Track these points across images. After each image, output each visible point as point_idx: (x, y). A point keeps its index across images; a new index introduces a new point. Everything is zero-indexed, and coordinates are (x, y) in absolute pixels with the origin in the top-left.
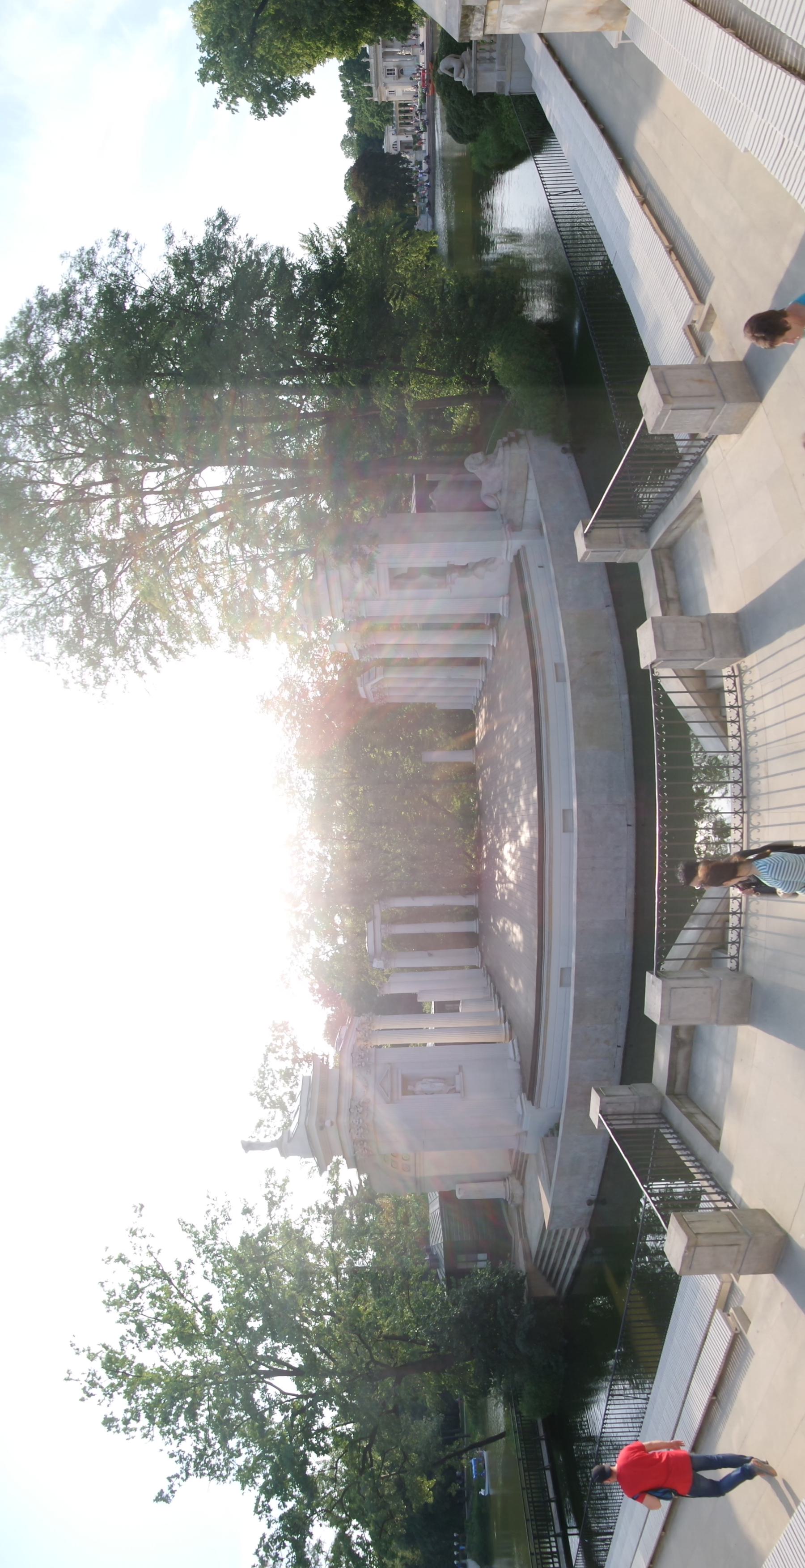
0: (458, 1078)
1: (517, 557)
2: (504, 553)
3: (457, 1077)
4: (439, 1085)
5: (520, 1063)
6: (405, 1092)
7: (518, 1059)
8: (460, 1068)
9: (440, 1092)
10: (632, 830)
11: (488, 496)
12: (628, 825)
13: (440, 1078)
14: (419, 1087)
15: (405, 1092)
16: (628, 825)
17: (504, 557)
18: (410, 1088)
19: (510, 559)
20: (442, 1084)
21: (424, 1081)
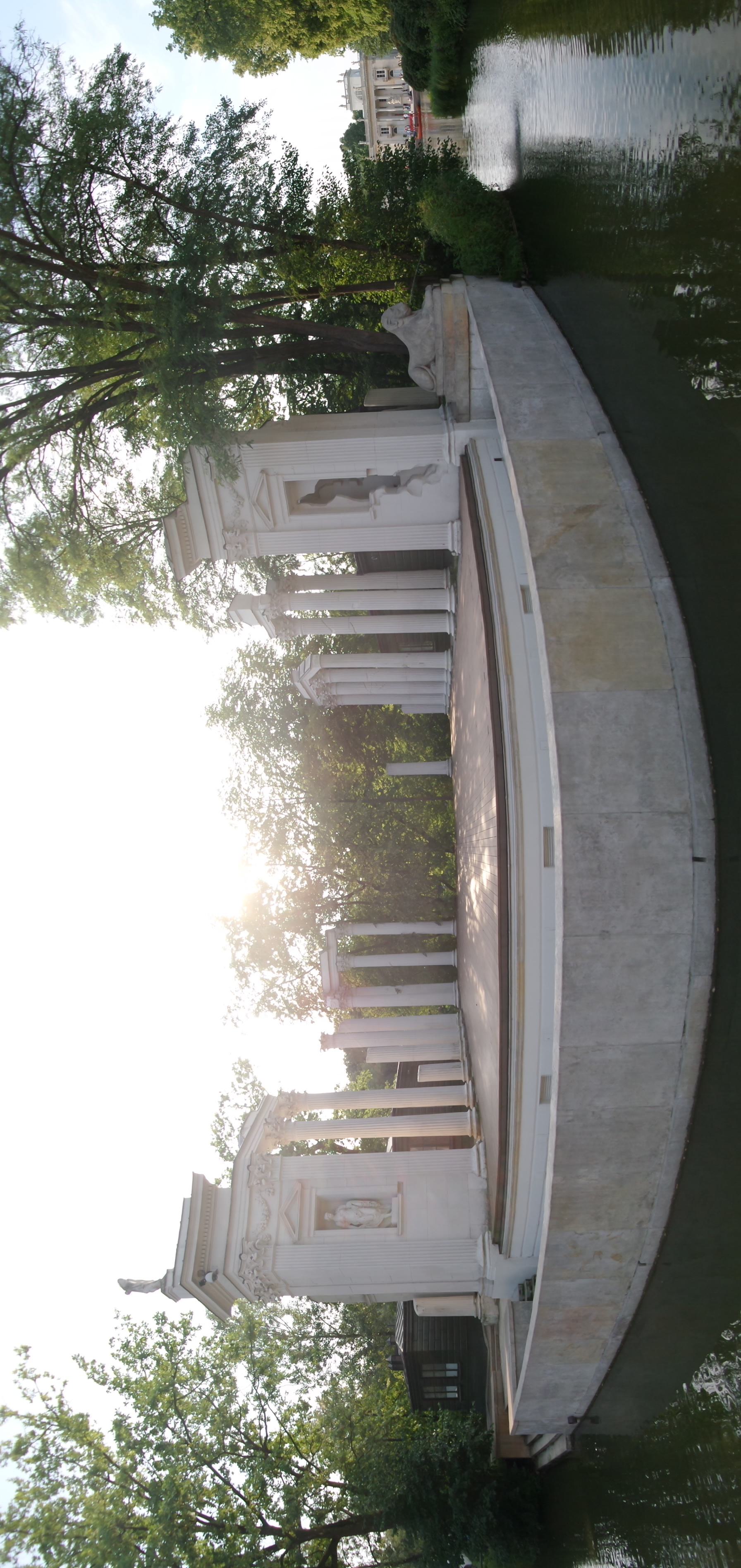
1: (465, 459)
2: (445, 452)
3: (395, 1200)
4: (369, 1214)
5: (487, 1179)
7: (484, 1175)
9: (369, 1225)
10: (707, 870)
11: (419, 368)
12: (696, 859)
13: (370, 1200)
15: (322, 1225)
16: (696, 859)
17: (447, 459)
18: (328, 1216)
19: (457, 461)
20: (373, 1211)
21: (349, 1204)
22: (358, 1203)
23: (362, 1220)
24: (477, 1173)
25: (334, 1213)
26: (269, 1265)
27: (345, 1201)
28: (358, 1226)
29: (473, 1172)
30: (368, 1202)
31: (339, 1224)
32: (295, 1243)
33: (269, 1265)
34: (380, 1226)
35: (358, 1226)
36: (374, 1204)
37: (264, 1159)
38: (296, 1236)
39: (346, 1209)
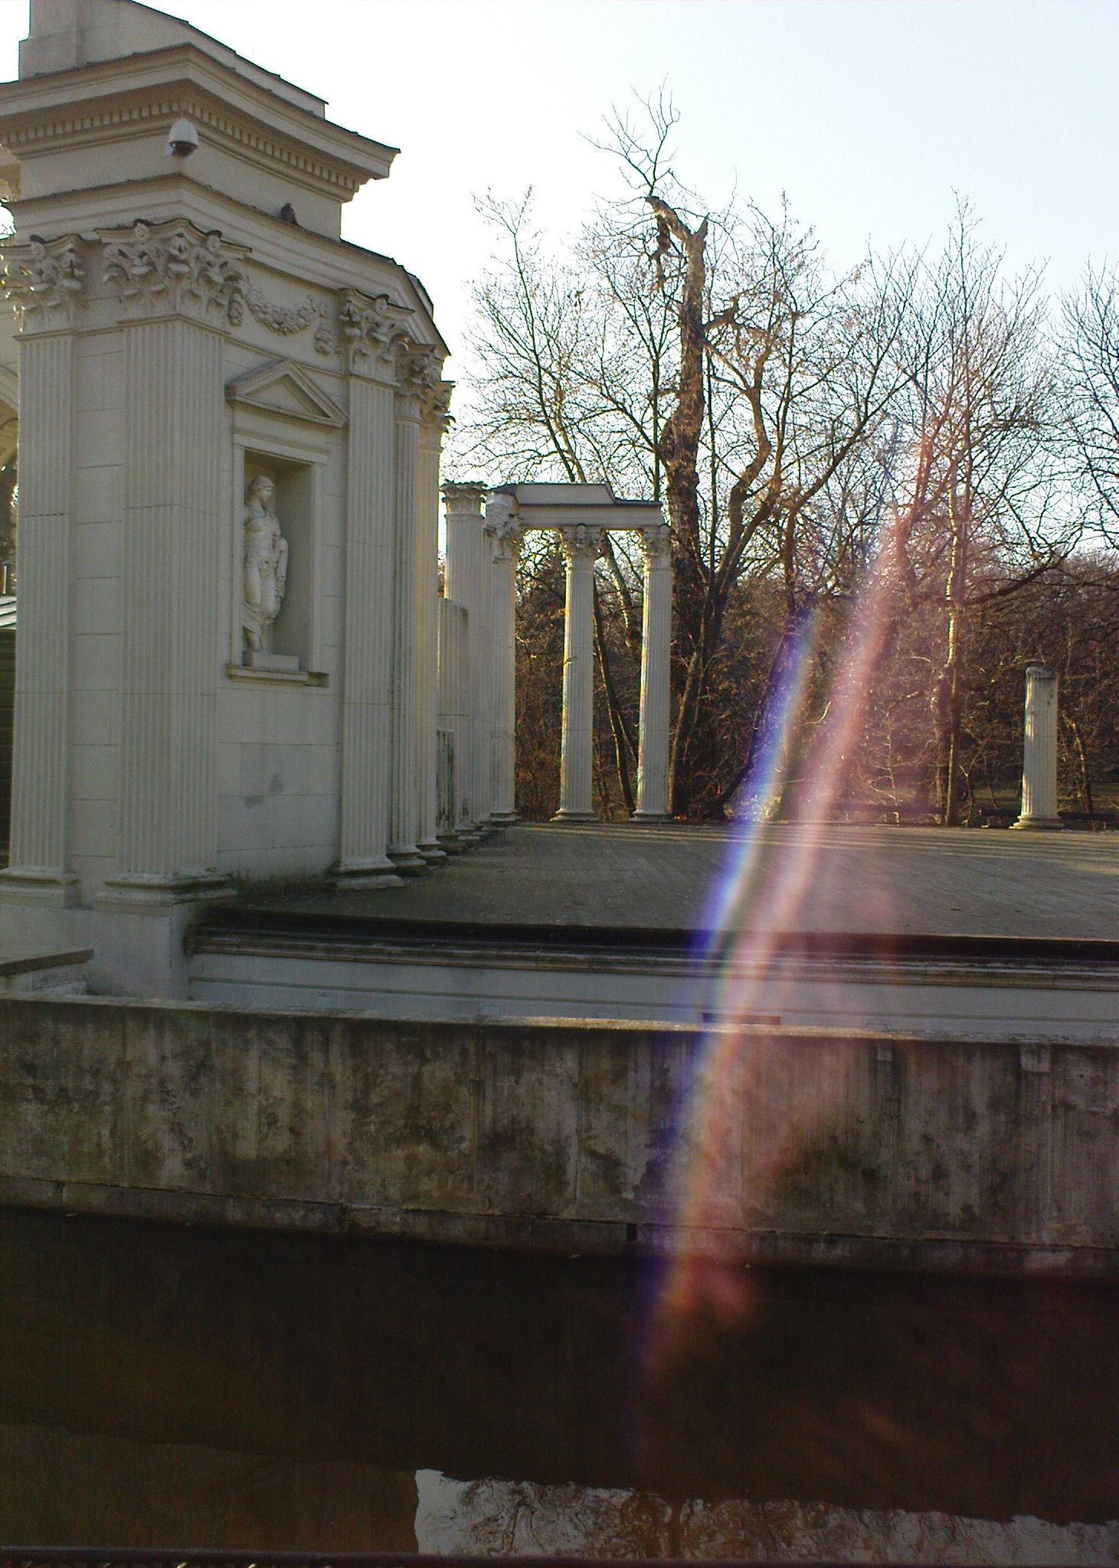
4: (267, 595)
6: (257, 463)
8: (320, 678)
21: (283, 544)
26: (191, 310)
32: (230, 390)
33: (191, 310)
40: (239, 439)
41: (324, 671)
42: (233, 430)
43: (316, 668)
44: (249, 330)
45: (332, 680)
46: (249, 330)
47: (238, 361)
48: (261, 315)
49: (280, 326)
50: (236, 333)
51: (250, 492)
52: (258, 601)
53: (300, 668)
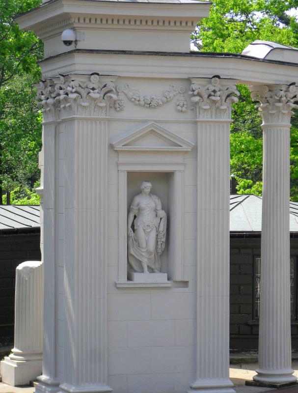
0: (161, 278)
6: (135, 180)
8: (185, 284)
14: (148, 204)
15: (135, 180)
20: (152, 247)
21: (162, 214)
22: (163, 228)
23: (141, 233)
24: (195, 385)
25: (152, 192)
27: (168, 209)
28: (133, 226)
29: (194, 379)
30: (164, 240)
31: (137, 199)
32: (111, 147)
34: (129, 255)
35: (133, 226)
36: (162, 247)
37: (228, 96)
38: (119, 147)
39: (156, 210)
40: (121, 168)
41: (186, 280)
42: (118, 165)
43: (178, 277)
44: (131, 112)
45: (190, 284)
46: (131, 112)
47: (120, 132)
48: (137, 102)
49: (149, 105)
50: (123, 115)
51: (134, 193)
52: (144, 245)
53: (169, 279)
